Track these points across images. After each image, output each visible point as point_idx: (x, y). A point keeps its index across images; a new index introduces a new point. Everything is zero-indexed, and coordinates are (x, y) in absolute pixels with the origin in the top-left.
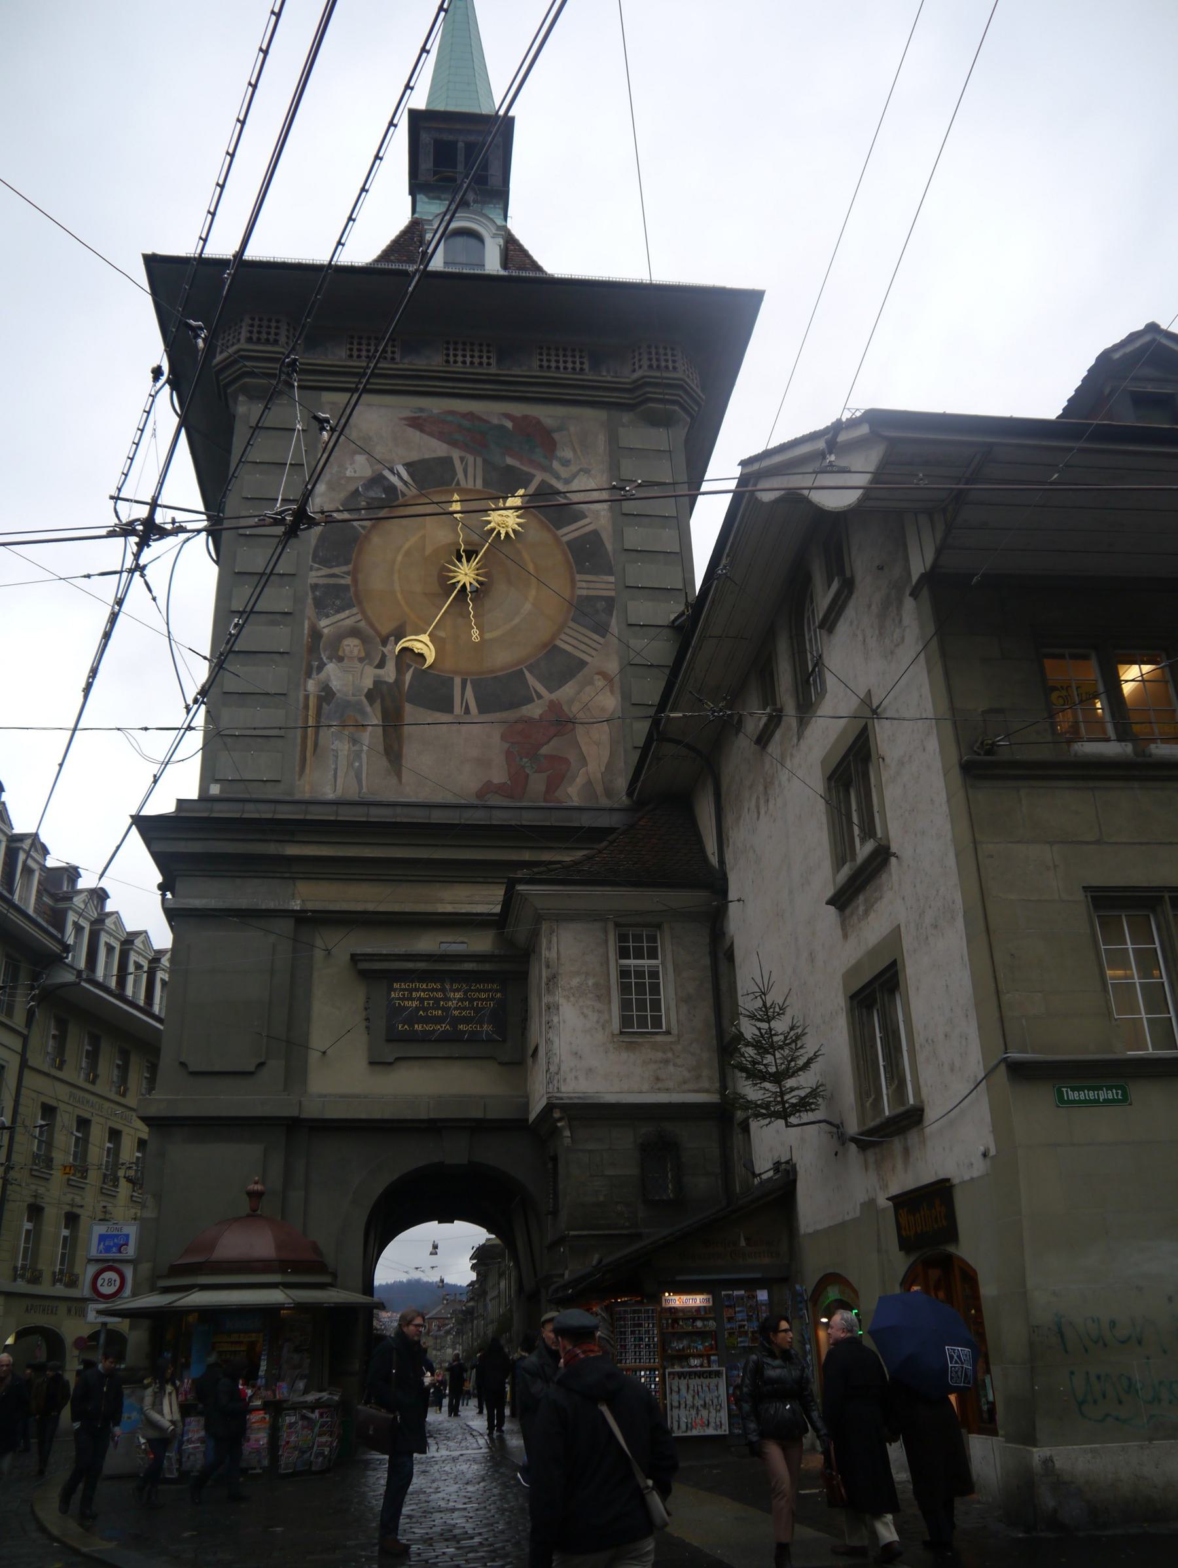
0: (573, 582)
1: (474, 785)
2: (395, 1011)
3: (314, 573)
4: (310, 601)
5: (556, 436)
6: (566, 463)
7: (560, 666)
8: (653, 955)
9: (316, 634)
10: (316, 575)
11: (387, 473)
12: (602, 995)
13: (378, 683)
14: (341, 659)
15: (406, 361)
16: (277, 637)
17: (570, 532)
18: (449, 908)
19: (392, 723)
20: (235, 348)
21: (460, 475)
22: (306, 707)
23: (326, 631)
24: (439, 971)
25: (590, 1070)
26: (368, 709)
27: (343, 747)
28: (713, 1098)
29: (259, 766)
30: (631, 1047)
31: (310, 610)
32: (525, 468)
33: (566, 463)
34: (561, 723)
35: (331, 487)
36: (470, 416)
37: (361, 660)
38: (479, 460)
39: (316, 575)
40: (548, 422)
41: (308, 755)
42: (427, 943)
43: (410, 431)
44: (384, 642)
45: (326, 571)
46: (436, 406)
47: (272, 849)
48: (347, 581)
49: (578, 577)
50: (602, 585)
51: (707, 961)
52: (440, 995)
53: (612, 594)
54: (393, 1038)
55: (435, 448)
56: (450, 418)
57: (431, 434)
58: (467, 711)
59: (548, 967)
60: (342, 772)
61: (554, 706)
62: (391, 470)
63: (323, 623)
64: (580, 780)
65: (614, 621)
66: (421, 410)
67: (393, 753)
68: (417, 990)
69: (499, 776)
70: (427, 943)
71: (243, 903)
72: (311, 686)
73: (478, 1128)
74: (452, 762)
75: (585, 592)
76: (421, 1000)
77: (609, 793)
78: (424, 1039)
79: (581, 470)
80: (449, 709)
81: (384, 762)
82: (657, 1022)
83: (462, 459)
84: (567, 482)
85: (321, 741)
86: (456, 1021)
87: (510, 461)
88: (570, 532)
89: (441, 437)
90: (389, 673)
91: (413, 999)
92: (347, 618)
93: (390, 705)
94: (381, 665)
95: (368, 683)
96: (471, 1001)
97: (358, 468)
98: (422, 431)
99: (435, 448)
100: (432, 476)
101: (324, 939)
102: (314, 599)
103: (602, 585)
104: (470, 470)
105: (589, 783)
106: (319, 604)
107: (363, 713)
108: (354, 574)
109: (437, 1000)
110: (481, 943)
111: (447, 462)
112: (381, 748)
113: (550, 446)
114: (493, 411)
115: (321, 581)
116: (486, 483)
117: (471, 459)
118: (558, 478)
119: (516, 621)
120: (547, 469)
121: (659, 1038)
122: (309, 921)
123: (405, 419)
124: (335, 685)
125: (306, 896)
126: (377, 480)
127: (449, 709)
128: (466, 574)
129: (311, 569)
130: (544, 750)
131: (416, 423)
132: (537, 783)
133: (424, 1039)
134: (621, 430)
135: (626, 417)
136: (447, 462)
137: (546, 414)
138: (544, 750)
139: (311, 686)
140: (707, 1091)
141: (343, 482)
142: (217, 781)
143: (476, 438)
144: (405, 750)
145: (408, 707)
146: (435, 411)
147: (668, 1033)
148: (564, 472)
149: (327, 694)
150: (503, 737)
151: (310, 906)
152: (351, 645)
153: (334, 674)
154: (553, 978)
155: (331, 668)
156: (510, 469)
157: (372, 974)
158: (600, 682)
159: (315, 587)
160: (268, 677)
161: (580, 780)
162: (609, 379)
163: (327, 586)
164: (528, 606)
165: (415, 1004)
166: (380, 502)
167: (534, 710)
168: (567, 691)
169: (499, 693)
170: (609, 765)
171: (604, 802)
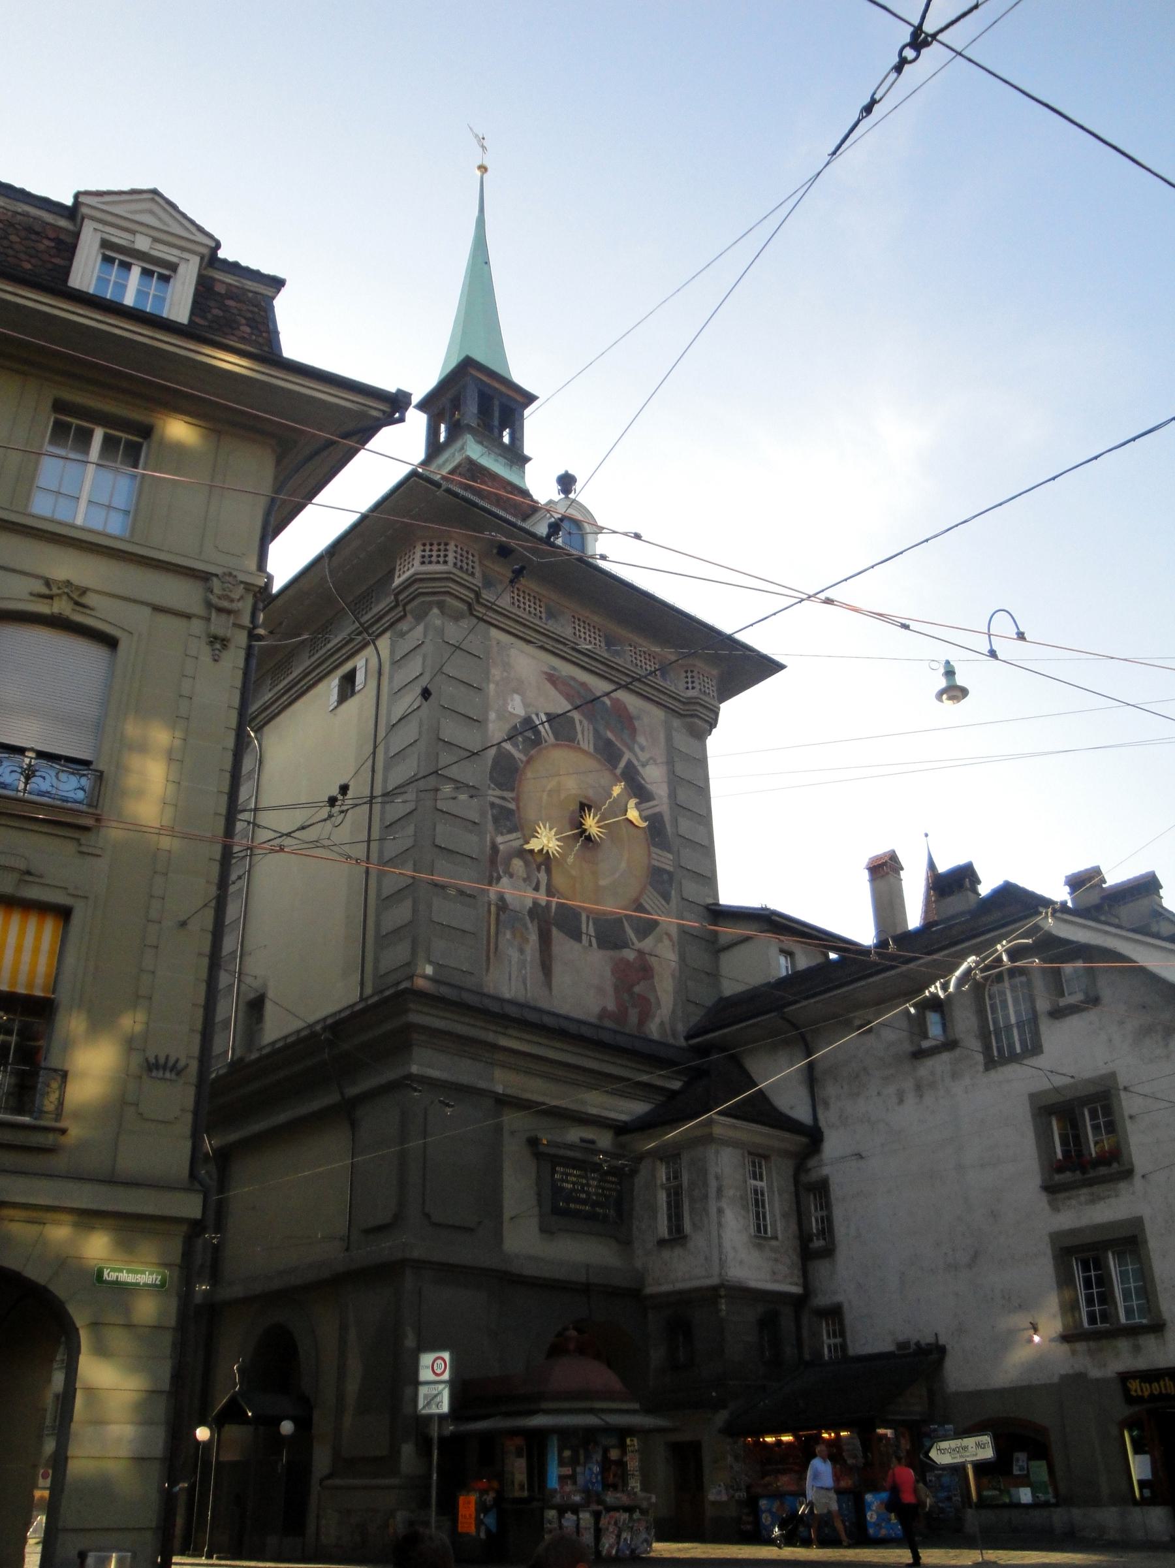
0: (649, 855)
1: (596, 1010)
2: (557, 1191)
3: (490, 792)
4: (490, 817)
5: (636, 723)
6: (642, 749)
8: (761, 1180)
9: (495, 848)
10: (493, 794)
11: (534, 717)
12: (745, 1208)
13: (536, 903)
14: (511, 876)
15: (550, 622)
16: (468, 842)
18: (594, 1111)
20: (440, 568)
21: (580, 736)
22: (489, 911)
23: (501, 847)
24: (582, 1160)
25: (741, 1262)
26: (530, 925)
27: (514, 955)
28: (796, 1290)
30: (759, 1247)
31: (490, 826)
32: (619, 745)
33: (642, 749)
34: (644, 969)
35: (500, 717)
37: (525, 880)
38: (591, 728)
40: (631, 709)
41: (492, 955)
43: (548, 686)
44: (539, 870)
45: (498, 793)
47: (490, 1037)
48: (512, 806)
49: (653, 849)
51: (792, 1188)
52: (584, 1181)
53: (671, 869)
54: (556, 1211)
56: (572, 683)
57: (561, 693)
58: (591, 945)
59: (717, 1178)
61: (641, 953)
62: (537, 715)
63: (499, 839)
64: (657, 1020)
65: (673, 892)
66: (554, 669)
67: (546, 966)
68: (571, 1175)
69: (611, 1006)
71: (464, 1079)
75: (656, 863)
76: (574, 1183)
77: (674, 1034)
78: (576, 1214)
79: (651, 758)
80: (579, 940)
81: (540, 975)
82: (766, 1232)
83: (581, 722)
84: (644, 766)
85: (500, 946)
86: (595, 1204)
87: (610, 735)
89: (568, 697)
90: (542, 897)
91: (567, 1182)
94: (537, 889)
95: (529, 904)
96: (603, 1189)
97: (517, 707)
98: (556, 689)
102: (493, 816)
103: (665, 860)
104: (586, 733)
105: (662, 1024)
106: (496, 820)
107: (525, 925)
108: (517, 800)
109: (583, 1185)
112: (538, 961)
113: (633, 731)
115: (497, 801)
116: (595, 749)
117: (585, 723)
118: (638, 760)
119: (617, 875)
120: (631, 750)
121: (774, 1243)
122: (503, 1102)
123: (546, 673)
124: (508, 897)
125: (502, 1081)
126: (528, 724)
127: (579, 940)
129: (489, 787)
130: (637, 989)
131: (552, 679)
132: (633, 1016)
133: (576, 1214)
134: (674, 733)
135: (676, 723)
138: (637, 989)
140: (796, 1284)
141: (507, 714)
142: (430, 962)
144: (554, 966)
145: (555, 932)
146: (564, 673)
147: (775, 1238)
148: (643, 756)
149: (502, 905)
150: (613, 972)
151: (509, 1091)
152: (517, 864)
154: (720, 1190)
155: (505, 880)
158: (667, 942)
159: (493, 805)
161: (657, 1020)
162: (673, 689)
163: (502, 808)
164: (623, 865)
165: (570, 1186)
167: (629, 955)
168: (647, 944)
169: (610, 935)
170: (674, 1012)
171: (671, 1041)
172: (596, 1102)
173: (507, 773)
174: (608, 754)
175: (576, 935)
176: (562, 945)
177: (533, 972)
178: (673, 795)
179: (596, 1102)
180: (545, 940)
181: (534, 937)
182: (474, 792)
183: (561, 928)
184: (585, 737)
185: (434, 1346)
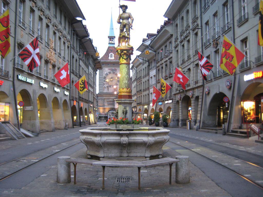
10: (104, 80)
16: (102, 84)
19: (108, 88)
24: (110, 101)
29: (101, 91)
36: (112, 69)
39: (104, 80)
42: (109, 100)
46: (110, 68)
55: (110, 71)
60: (106, 91)
72: (104, 86)
73: (112, 108)
90: (108, 85)
93: (108, 87)
97: (106, 73)
99: (110, 71)
101: (105, 99)
111: (110, 72)
114: (113, 68)
122: (104, 99)
125: (104, 98)
126: (107, 73)
128: (112, 80)
131: (109, 69)
136: (110, 72)
137: (116, 68)
139: (104, 86)
143: (112, 70)
149: (105, 87)
152: (106, 84)
155: (105, 85)
156: (114, 72)
157: (108, 101)
160: (101, 86)
166: (107, 74)
172: (111, 98)
173: (105, 78)
174: (114, 73)
175: (111, 87)
176: (109, 88)
177: (107, 90)
179: (111, 98)
180: (108, 88)
181: (107, 88)
182: (102, 80)
183: (109, 87)
184: (112, 73)
185: (75, 116)
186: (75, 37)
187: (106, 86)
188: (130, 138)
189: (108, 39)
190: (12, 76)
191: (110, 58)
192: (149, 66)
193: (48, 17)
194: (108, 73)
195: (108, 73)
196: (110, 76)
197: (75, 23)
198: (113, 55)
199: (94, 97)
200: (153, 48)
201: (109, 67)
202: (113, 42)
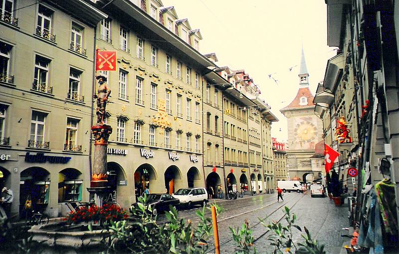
7: (313, 138)
17: (314, 127)
19: (301, 144)
50: (316, 131)
55: (302, 121)
67: (301, 146)
70: (305, 159)
74: (306, 146)
88: (314, 127)
92: (297, 136)
99: (302, 121)
100: (302, 123)
103: (316, 131)
110: (309, 159)
114: (307, 117)
132: (312, 147)
143: (305, 119)
153: (296, 141)
173: (296, 130)
174: (308, 123)
178: (318, 125)
180: (301, 144)
184: (305, 122)
186: (213, 89)
187: (298, 140)
188: (57, 240)
189: (299, 78)
190: (88, 150)
191: (301, 104)
192: (330, 113)
193: (153, 75)
194: (300, 124)
195: (300, 124)
196: (302, 127)
197: (206, 74)
198: (306, 99)
199: (263, 158)
200: (329, 89)
201: (301, 115)
202: (306, 82)
